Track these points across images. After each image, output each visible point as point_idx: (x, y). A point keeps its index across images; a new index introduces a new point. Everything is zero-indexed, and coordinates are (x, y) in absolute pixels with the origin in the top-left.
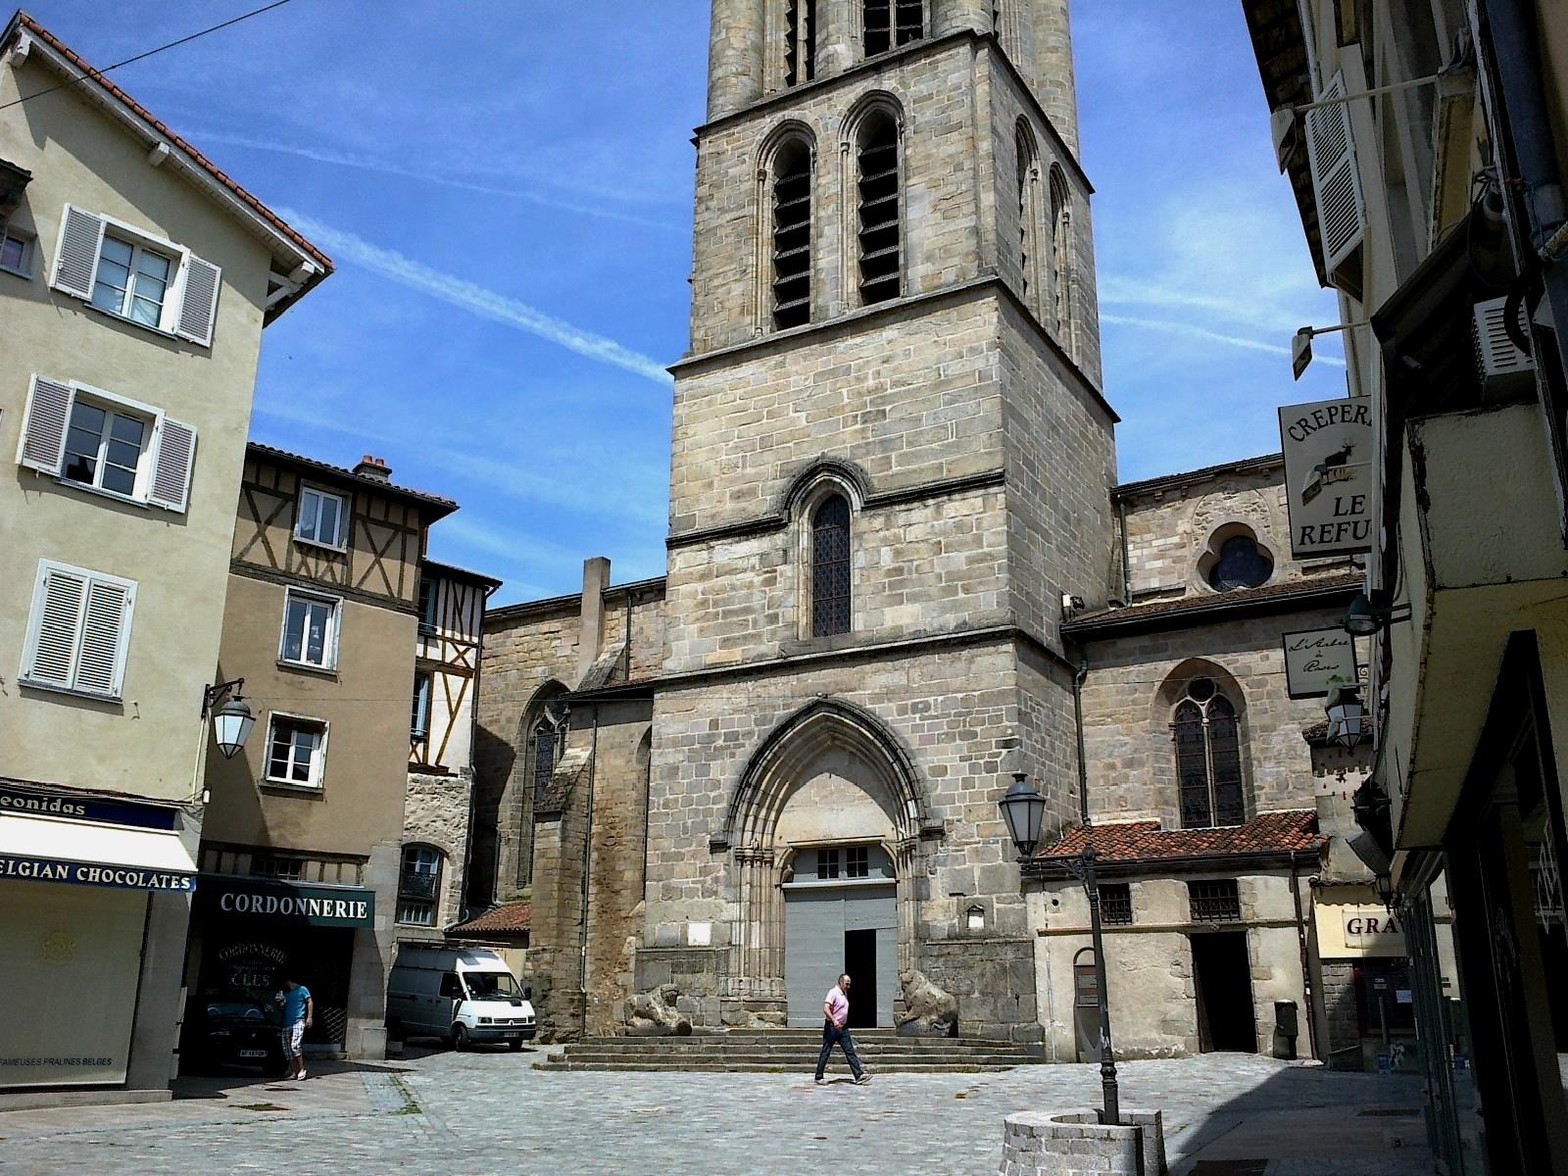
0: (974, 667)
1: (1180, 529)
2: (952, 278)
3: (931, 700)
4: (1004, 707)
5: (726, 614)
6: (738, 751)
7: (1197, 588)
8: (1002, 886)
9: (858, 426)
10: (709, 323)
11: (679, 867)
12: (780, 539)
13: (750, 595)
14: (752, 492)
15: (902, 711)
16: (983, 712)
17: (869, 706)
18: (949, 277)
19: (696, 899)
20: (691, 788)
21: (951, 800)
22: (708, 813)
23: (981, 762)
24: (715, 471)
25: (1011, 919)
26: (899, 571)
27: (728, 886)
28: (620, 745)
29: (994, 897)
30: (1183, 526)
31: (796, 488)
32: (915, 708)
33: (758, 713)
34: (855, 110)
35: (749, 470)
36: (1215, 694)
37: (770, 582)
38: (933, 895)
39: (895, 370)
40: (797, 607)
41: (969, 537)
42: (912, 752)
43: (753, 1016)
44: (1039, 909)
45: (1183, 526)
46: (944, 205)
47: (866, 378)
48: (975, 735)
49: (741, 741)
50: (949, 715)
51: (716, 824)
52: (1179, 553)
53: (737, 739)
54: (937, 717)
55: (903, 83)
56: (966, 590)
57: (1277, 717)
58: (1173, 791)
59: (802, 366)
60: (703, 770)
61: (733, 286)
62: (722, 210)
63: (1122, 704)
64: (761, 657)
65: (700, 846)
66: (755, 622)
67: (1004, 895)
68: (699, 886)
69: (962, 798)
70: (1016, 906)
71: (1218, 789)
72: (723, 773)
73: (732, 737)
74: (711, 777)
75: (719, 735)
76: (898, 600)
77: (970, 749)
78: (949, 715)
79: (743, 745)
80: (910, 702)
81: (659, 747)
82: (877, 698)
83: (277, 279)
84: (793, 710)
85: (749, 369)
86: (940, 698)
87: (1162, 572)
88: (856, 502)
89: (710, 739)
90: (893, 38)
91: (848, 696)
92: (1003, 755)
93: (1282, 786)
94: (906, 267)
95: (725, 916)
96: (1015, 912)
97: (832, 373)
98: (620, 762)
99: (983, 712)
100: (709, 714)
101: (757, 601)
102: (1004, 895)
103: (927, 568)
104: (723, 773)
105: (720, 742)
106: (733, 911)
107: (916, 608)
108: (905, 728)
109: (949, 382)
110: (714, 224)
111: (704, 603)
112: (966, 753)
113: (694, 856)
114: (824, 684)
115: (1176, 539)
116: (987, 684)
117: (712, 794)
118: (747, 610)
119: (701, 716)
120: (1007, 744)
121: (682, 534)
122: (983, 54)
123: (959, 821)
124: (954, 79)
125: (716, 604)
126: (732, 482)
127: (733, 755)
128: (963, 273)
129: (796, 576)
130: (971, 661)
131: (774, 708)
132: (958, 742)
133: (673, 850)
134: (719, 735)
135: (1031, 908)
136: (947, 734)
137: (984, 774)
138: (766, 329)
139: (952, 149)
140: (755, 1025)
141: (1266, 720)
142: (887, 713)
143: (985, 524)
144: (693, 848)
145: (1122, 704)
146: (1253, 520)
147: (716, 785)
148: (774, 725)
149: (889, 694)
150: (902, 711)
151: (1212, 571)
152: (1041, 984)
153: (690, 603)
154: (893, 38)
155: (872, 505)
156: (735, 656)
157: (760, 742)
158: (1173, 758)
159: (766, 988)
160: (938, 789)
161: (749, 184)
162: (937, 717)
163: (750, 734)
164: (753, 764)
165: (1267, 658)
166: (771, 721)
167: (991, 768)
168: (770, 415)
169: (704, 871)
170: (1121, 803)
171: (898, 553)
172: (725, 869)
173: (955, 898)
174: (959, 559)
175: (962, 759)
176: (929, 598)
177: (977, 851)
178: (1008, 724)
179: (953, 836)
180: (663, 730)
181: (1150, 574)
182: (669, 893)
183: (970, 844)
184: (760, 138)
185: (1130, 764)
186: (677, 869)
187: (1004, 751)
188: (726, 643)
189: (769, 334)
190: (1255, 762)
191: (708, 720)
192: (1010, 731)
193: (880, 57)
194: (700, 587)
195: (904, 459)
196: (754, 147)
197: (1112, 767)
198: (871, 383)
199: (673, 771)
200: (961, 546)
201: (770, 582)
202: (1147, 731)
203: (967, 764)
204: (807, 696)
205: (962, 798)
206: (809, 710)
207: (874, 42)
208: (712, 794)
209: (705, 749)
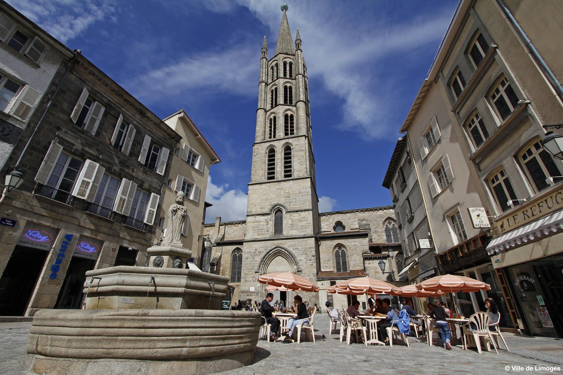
1: (330, 221)
2: (302, 175)
3: (299, 247)
5: (258, 229)
7: (333, 231)
9: (285, 198)
10: (256, 177)
12: (269, 216)
13: (263, 227)
14: (264, 208)
15: (294, 249)
18: (301, 175)
20: (251, 261)
22: (254, 266)
24: (256, 203)
26: (293, 224)
28: (227, 253)
30: (331, 221)
31: (273, 208)
32: (296, 249)
33: (265, 248)
34: (284, 145)
35: (263, 204)
37: (267, 224)
39: (292, 190)
40: (272, 229)
41: (306, 219)
44: (319, 284)
45: (331, 221)
46: (301, 163)
47: (286, 190)
48: (307, 254)
51: (256, 268)
52: (330, 225)
55: (293, 141)
56: (305, 229)
57: (353, 254)
58: (335, 265)
59: (273, 187)
60: (254, 258)
61: (261, 171)
62: (259, 158)
63: (327, 250)
64: (265, 238)
66: (264, 232)
71: (343, 265)
72: (258, 258)
73: (260, 252)
76: (292, 229)
82: (289, 247)
83: (212, 162)
85: (264, 186)
87: (327, 228)
88: (284, 212)
89: (255, 252)
90: (289, 133)
91: (283, 246)
93: (354, 265)
94: (293, 172)
97: (280, 189)
98: (227, 256)
101: (265, 227)
103: (298, 224)
104: (258, 258)
105: (257, 253)
107: (296, 231)
108: (294, 252)
109: (302, 193)
110: (257, 160)
111: (254, 227)
112: (306, 257)
113: (251, 274)
115: (329, 223)
118: (263, 229)
120: (313, 256)
121: (249, 214)
122: (307, 138)
124: (302, 142)
125: (256, 227)
126: (260, 206)
127: (260, 256)
128: (304, 175)
129: (272, 224)
130: (306, 241)
131: (268, 247)
138: (266, 179)
139: (302, 154)
141: (351, 254)
142: (291, 249)
143: (309, 217)
145: (327, 250)
146: (342, 221)
147: (256, 261)
148: (268, 250)
149: (291, 246)
150: (294, 249)
151: (334, 228)
152: (320, 298)
153: (251, 227)
154: (289, 133)
155: (287, 212)
156: (260, 237)
157: (265, 254)
160: (300, 263)
161: (264, 154)
163: (263, 252)
167: (310, 260)
168: (268, 195)
169: (253, 277)
170: (327, 267)
171: (292, 221)
174: (304, 223)
176: (298, 230)
177: (308, 275)
179: (303, 272)
181: (325, 228)
182: (246, 281)
184: (266, 147)
185: (328, 261)
186: (248, 277)
188: (258, 235)
189: (266, 181)
193: (287, 137)
194: (253, 224)
195: (293, 205)
196: (265, 148)
197: (325, 261)
198: (287, 191)
199: (247, 258)
200: (304, 221)
201: (267, 224)
205: (305, 265)
207: (286, 134)
209: (254, 254)
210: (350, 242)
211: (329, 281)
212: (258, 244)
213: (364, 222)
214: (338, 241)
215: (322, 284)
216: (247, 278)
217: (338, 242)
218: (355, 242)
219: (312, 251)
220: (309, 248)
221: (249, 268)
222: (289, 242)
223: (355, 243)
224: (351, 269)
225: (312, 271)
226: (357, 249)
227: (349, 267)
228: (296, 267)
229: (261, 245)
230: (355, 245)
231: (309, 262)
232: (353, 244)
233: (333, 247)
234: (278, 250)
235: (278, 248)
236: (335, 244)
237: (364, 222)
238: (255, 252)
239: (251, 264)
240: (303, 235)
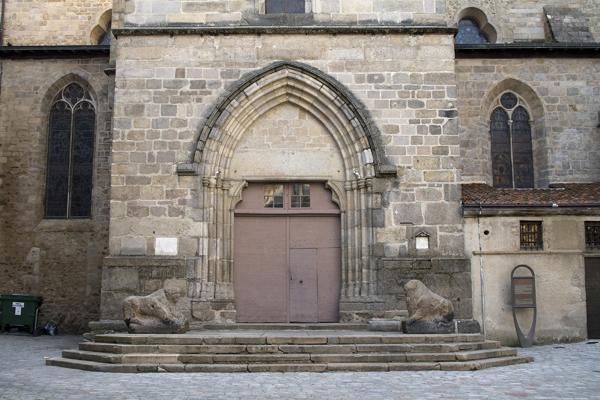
0: (420, 53)
3: (385, 73)
4: (446, 86)
6: (204, 98)
8: (444, 219)
11: (145, 189)
15: (360, 79)
16: (429, 88)
17: (330, 73)
19: (163, 217)
20: (156, 124)
21: (403, 151)
22: (174, 146)
23: (427, 125)
25: (451, 243)
27: (196, 208)
29: (438, 226)
32: (371, 79)
33: (225, 68)
36: (518, 105)
38: (386, 222)
42: (368, 112)
43: (217, 314)
44: (473, 235)
48: (421, 104)
49: (208, 89)
50: (400, 87)
51: (182, 155)
53: (204, 87)
54: (390, 88)
57: (564, 123)
60: (169, 110)
64: (225, 23)
65: (167, 172)
67: (446, 225)
68: (166, 206)
69: (412, 150)
70: (457, 234)
72: (189, 112)
74: (177, 117)
75: (186, 83)
77: (417, 115)
78: (400, 87)
79: (210, 93)
80: (366, 74)
81: (123, 86)
82: (337, 67)
84: (259, 68)
86: (393, 74)
89: (177, 84)
91: (311, 62)
92: (444, 123)
93: (566, 166)
95: (193, 233)
96: (456, 239)
99: (429, 88)
100: (175, 64)
102: (446, 225)
105: (187, 88)
106: (201, 229)
112: (414, 118)
113: (161, 180)
114: (288, 51)
116: (432, 68)
117: (179, 131)
119: (167, 65)
120: (449, 114)
123: (409, 168)
130: (418, 47)
132: (408, 108)
133: (139, 175)
134: (186, 83)
135: (467, 236)
136: (398, 102)
137: (429, 134)
140: (220, 322)
141: (557, 125)
144: (160, 173)
147: (183, 123)
149: (348, 65)
150: (360, 79)
158: (489, 143)
159: (225, 292)
160: (391, 143)
162: (390, 88)
163: (216, 84)
164: (220, 110)
165: (558, 84)
166: (238, 75)
167: (435, 130)
169: (171, 194)
172: (192, 194)
173: (405, 227)
175: (411, 122)
177: (423, 192)
178: (449, 99)
179: (403, 180)
180: (127, 73)
182: (134, 210)
183: (417, 185)
187: (446, 119)
190: (549, 151)
191: (174, 68)
192: (450, 105)
199: (138, 109)
202: (479, 124)
203: (415, 126)
204: (271, 58)
205: (412, 150)
206: (276, 68)
208: (179, 131)
210: (553, 79)
211: (516, 220)
212: (191, 49)
213: (567, 20)
214: (506, 70)
215: (486, 233)
216: (137, 195)
217: (506, 76)
218: (574, 78)
219: (441, 95)
220: (429, 78)
221: (151, 155)
222: (337, 45)
223: (571, 84)
224: (553, 179)
225: (443, 177)
226: (579, 107)
227: (547, 173)
228: (368, 156)
229: (207, 55)
230: (574, 92)
231: (428, 139)
232: (565, 84)
233: (487, 91)
234: (288, 78)
235: (287, 72)
236: (495, 82)
237: (567, 20)
238: (177, 84)
239: (155, 135)
240: (399, 20)
